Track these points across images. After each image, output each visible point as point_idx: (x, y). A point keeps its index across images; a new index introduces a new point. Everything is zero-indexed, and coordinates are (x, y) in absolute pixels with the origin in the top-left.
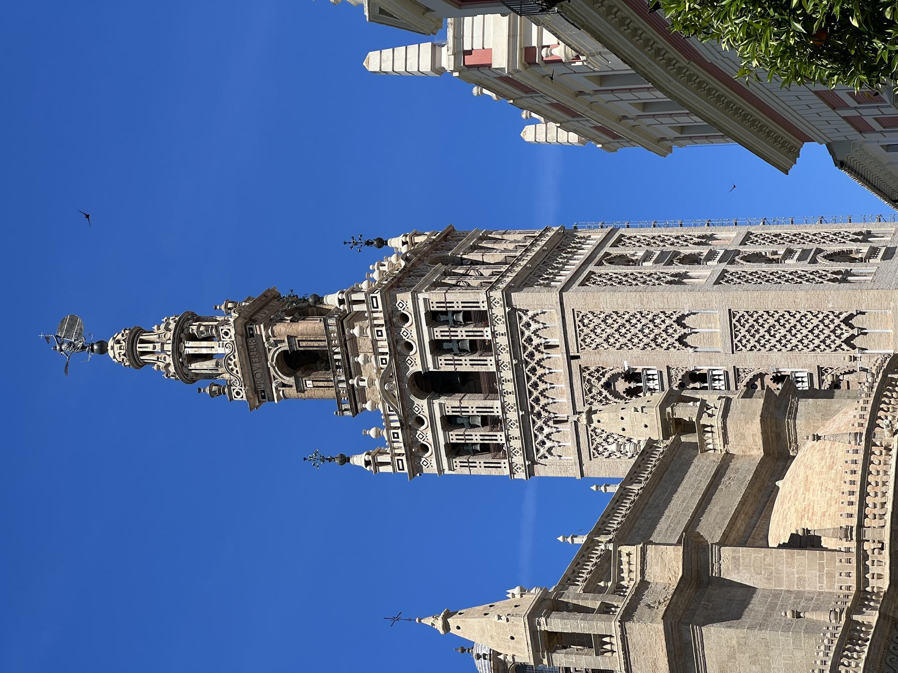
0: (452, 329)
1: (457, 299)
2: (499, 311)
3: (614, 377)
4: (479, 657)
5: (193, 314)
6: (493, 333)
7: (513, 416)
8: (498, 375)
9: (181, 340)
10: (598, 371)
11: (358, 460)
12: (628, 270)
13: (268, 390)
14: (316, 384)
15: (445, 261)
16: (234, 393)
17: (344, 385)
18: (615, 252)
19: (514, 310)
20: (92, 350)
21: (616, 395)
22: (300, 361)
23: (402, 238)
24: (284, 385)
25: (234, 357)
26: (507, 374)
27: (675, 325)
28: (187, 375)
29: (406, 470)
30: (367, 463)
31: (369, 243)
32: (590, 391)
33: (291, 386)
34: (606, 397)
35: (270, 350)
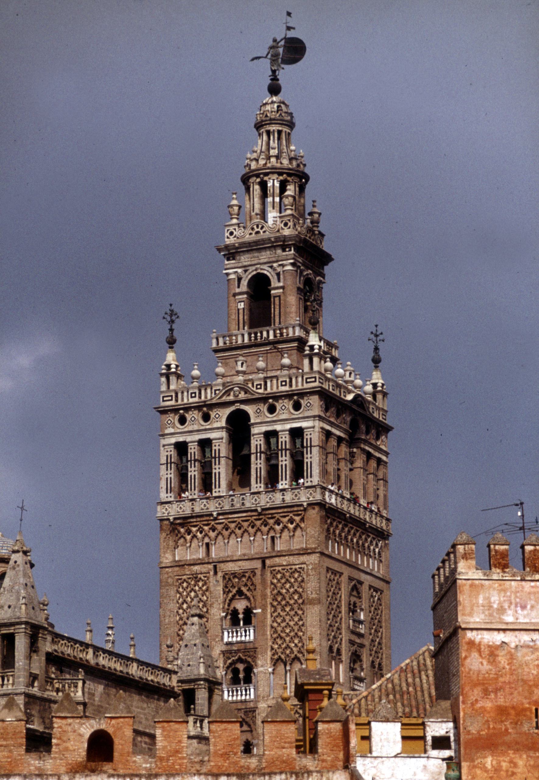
0: (288, 452)
1: (313, 458)
2: (304, 497)
9: (280, 174)
10: (253, 584)
11: (171, 358)
14: (241, 312)
16: (231, 229)
18: (364, 589)
19: (305, 510)
25: (264, 232)
28: (248, 180)
31: (376, 349)
32: (235, 577)
33: (239, 287)
34: (230, 591)
35: (271, 267)
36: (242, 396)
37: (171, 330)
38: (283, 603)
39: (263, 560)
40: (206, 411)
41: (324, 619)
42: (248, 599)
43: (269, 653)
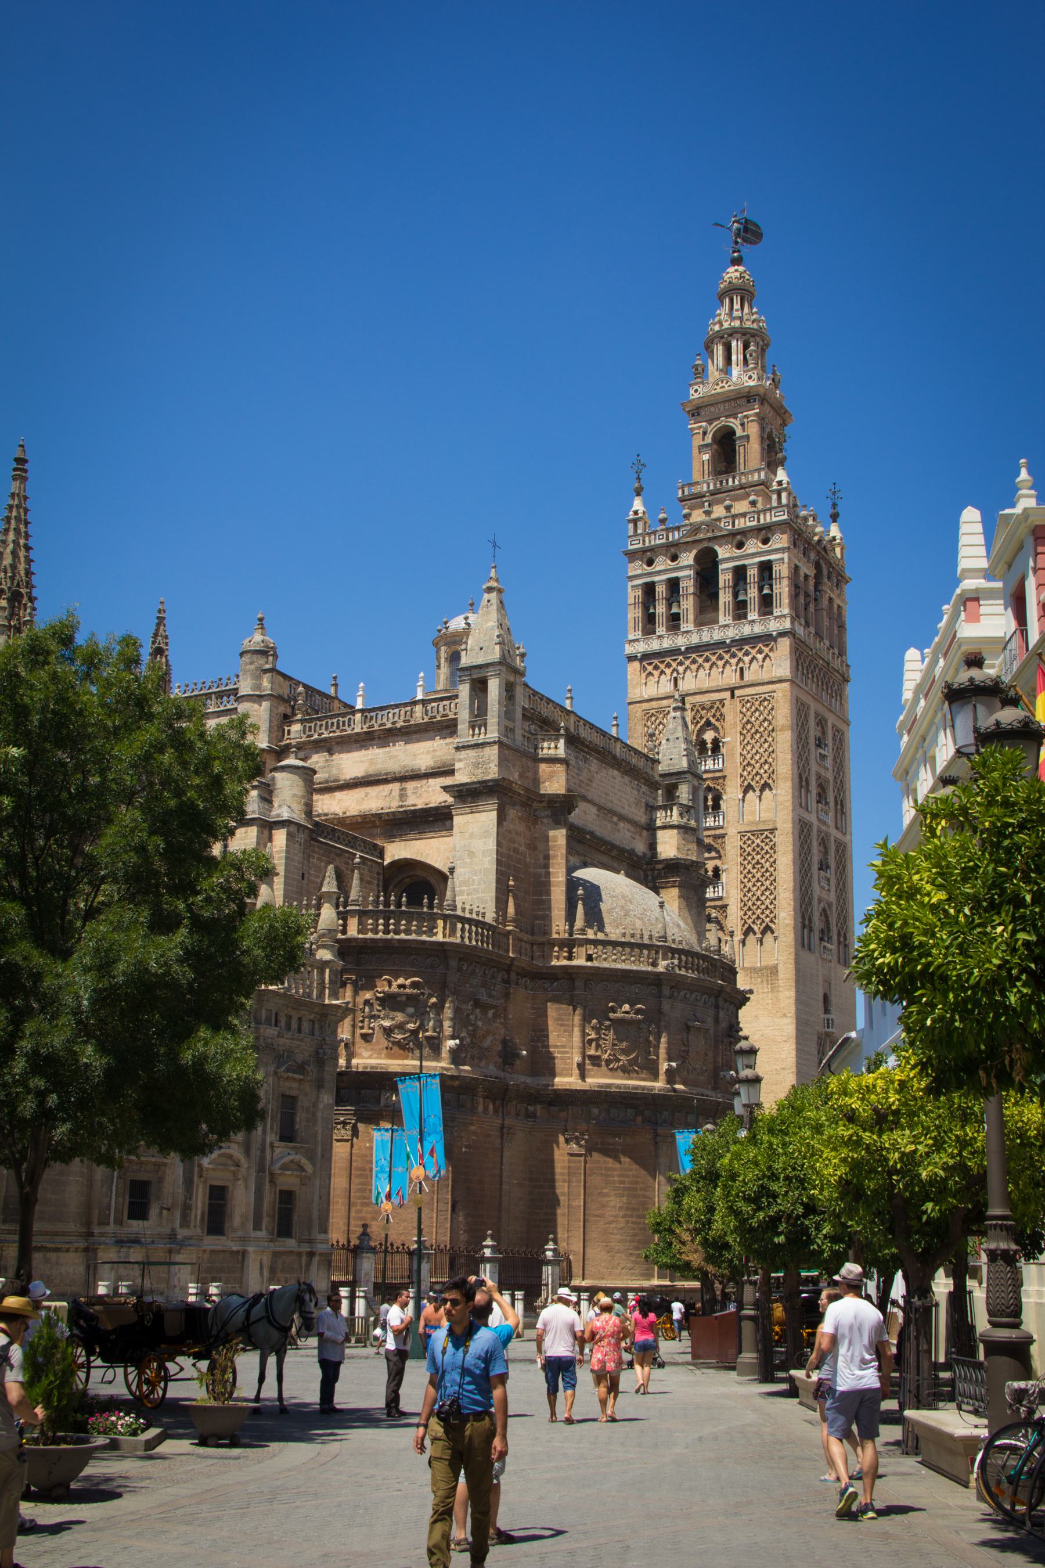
3: (716, 729)
4: (466, 618)
5: (767, 345)
6: (753, 621)
7: (681, 642)
8: (716, 627)
9: (744, 334)
10: (721, 715)
11: (638, 505)
12: (812, 742)
13: (699, 419)
15: (818, 576)
16: (696, 387)
17: (705, 489)
19: (775, 640)
20: (734, 252)
21: (701, 731)
22: (725, 448)
23: (838, 536)
24: (705, 433)
26: (717, 635)
27: (763, 782)
29: (630, 548)
30: (636, 513)
31: (834, 506)
32: (703, 709)
34: (698, 722)
36: (710, 535)
37: (639, 479)
38: (753, 730)
39: (732, 690)
40: (673, 552)
41: (795, 747)
42: (716, 729)
43: (739, 781)
